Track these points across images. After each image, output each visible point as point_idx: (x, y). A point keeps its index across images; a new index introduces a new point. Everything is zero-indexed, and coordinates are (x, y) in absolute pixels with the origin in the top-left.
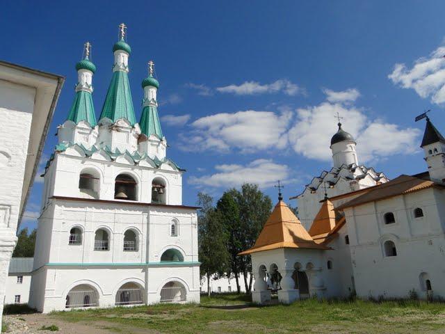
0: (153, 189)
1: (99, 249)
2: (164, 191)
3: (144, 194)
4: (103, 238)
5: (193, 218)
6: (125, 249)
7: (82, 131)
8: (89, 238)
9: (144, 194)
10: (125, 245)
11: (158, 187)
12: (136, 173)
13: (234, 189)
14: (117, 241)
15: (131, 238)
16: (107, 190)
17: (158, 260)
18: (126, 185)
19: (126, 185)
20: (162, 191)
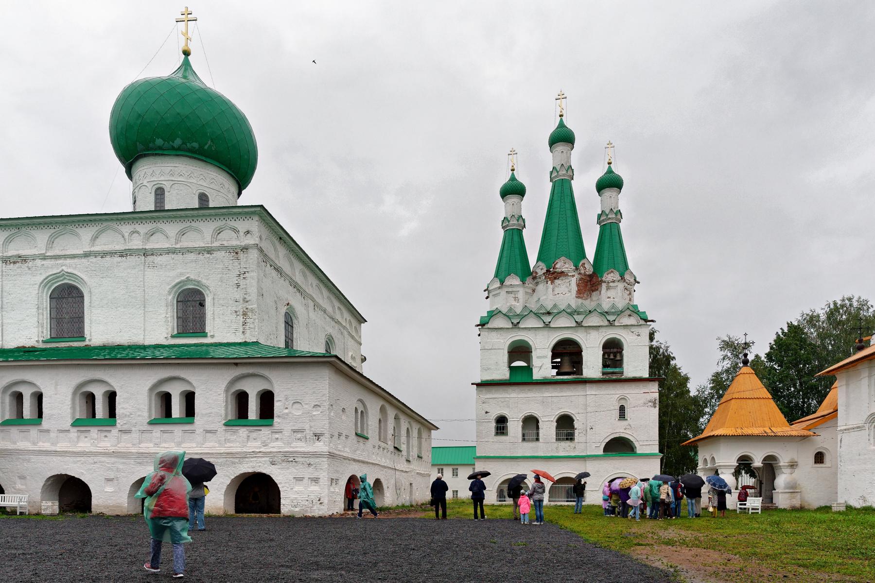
0: (604, 355)
1: (529, 441)
2: (622, 356)
3: (592, 364)
4: (531, 422)
5: (653, 391)
6: (524, 440)
7: (510, 290)
8: (515, 427)
9: (592, 364)
10: (557, 434)
11: (613, 352)
12: (578, 336)
13: (790, 326)
14: (548, 429)
15: (565, 425)
16: (543, 366)
17: (601, 452)
18: (567, 354)
19: (567, 354)
20: (618, 358)
